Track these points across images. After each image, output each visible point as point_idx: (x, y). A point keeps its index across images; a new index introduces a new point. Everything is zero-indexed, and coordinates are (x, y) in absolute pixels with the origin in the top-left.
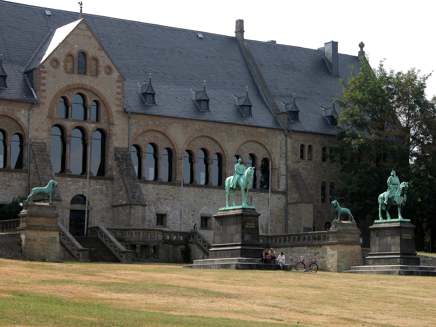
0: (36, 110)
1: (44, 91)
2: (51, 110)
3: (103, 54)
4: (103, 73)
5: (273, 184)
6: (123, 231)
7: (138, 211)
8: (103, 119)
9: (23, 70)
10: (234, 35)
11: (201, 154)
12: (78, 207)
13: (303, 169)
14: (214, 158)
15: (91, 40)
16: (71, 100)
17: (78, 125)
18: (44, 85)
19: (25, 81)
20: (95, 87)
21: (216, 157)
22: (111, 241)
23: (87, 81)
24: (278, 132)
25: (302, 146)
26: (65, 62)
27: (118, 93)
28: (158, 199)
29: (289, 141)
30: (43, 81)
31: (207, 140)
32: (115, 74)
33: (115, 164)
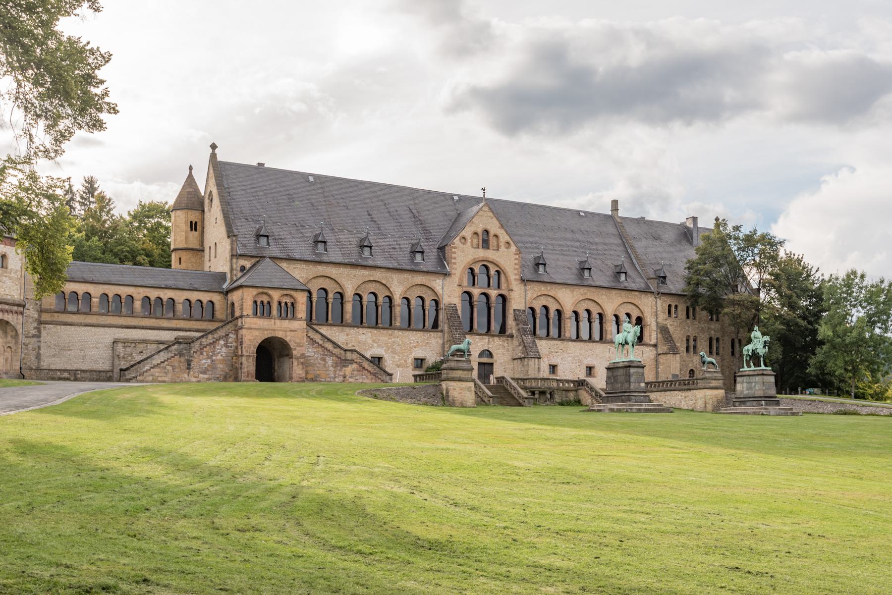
0: (448, 279)
1: (455, 263)
2: (461, 279)
3: (502, 231)
4: (503, 248)
5: (646, 339)
6: (523, 380)
7: (532, 363)
8: (504, 285)
9: (437, 246)
10: (610, 213)
11: (585, 315)
12: (485, 360)
14: (595, 316)
16: (477, 271)
17: (483, 291)
18: (455, 258)
19: (438, 255)
21: (598, 316)
22: (515, 389)
23: (490, 254)
24: (649, 295)
26: (471, 239)
28: (550, 352)
29: (659, 302)
30: (453, 255)
31: (590, 302)
32: (513, 248)
33: (514, 323)
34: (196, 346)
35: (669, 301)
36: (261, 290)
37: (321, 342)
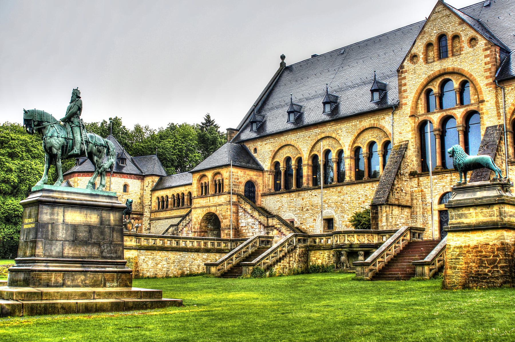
3: (465, 27)
15: (450, 17)
20: (459, 67)
23: (449, 64)
27: (486, 64)
34: (180, 227)
36: (201, 173)
37: (250, 211)
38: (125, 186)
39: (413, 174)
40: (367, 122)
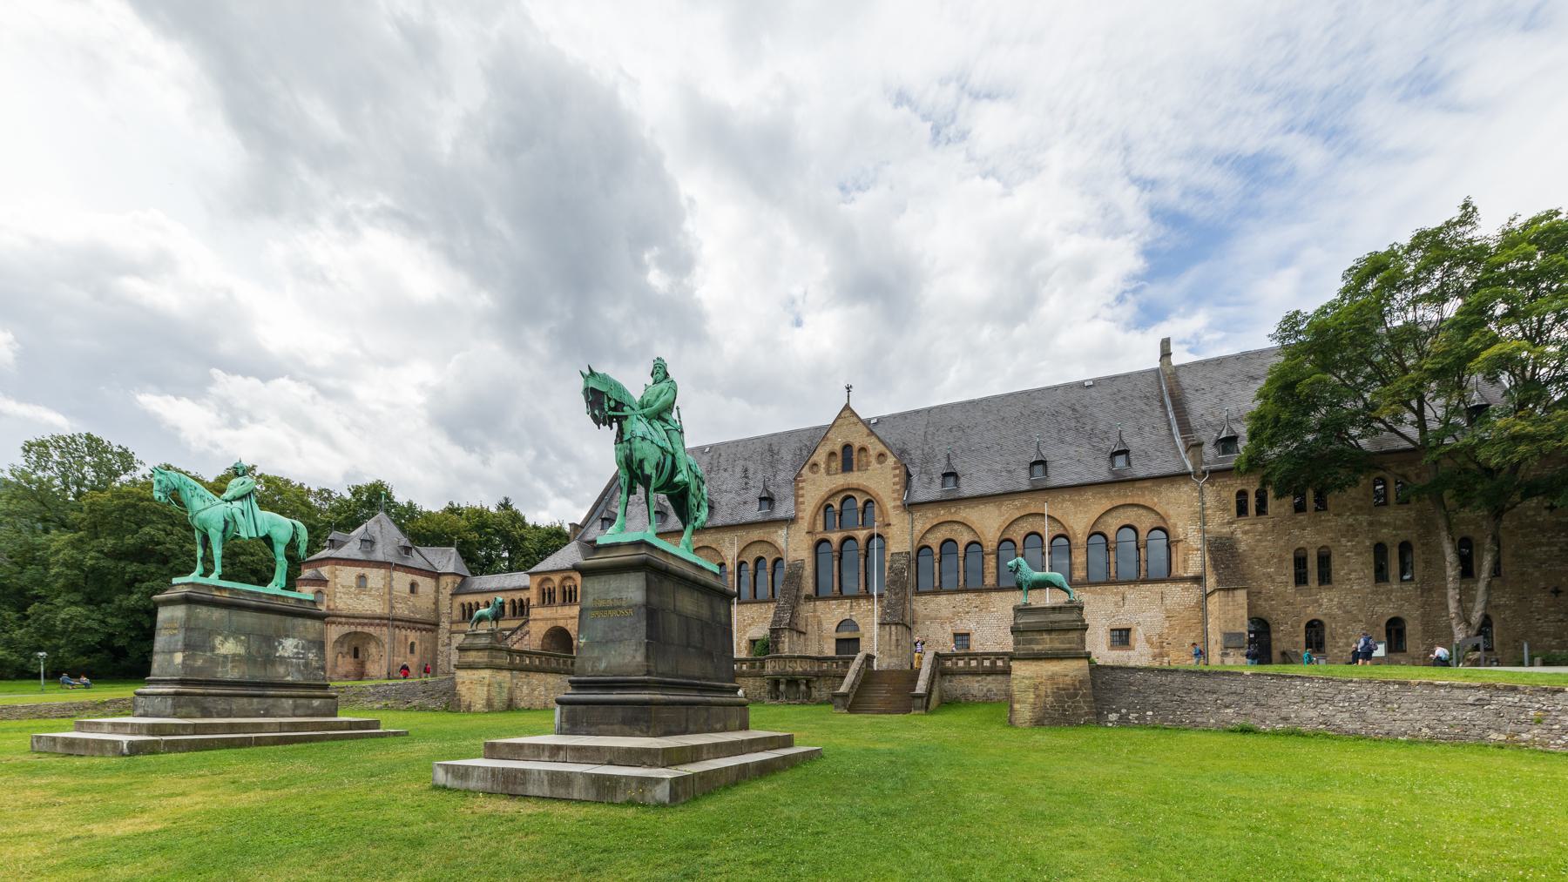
0: (793, 527)
12: (845, 635)
13: (1245, 533)
25: (1242, 495)
35: (1238, 484)
38: (413, 587)
39: (808, 598)
40: (756, 535)
